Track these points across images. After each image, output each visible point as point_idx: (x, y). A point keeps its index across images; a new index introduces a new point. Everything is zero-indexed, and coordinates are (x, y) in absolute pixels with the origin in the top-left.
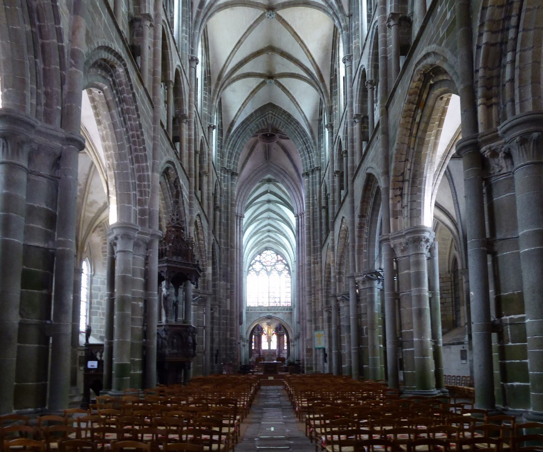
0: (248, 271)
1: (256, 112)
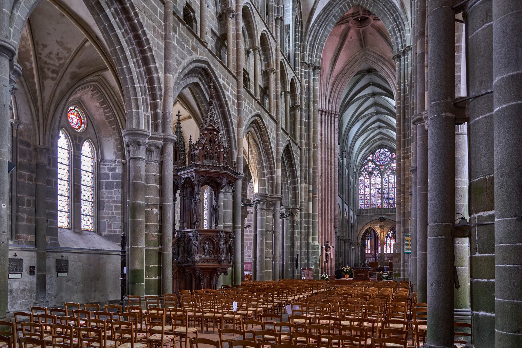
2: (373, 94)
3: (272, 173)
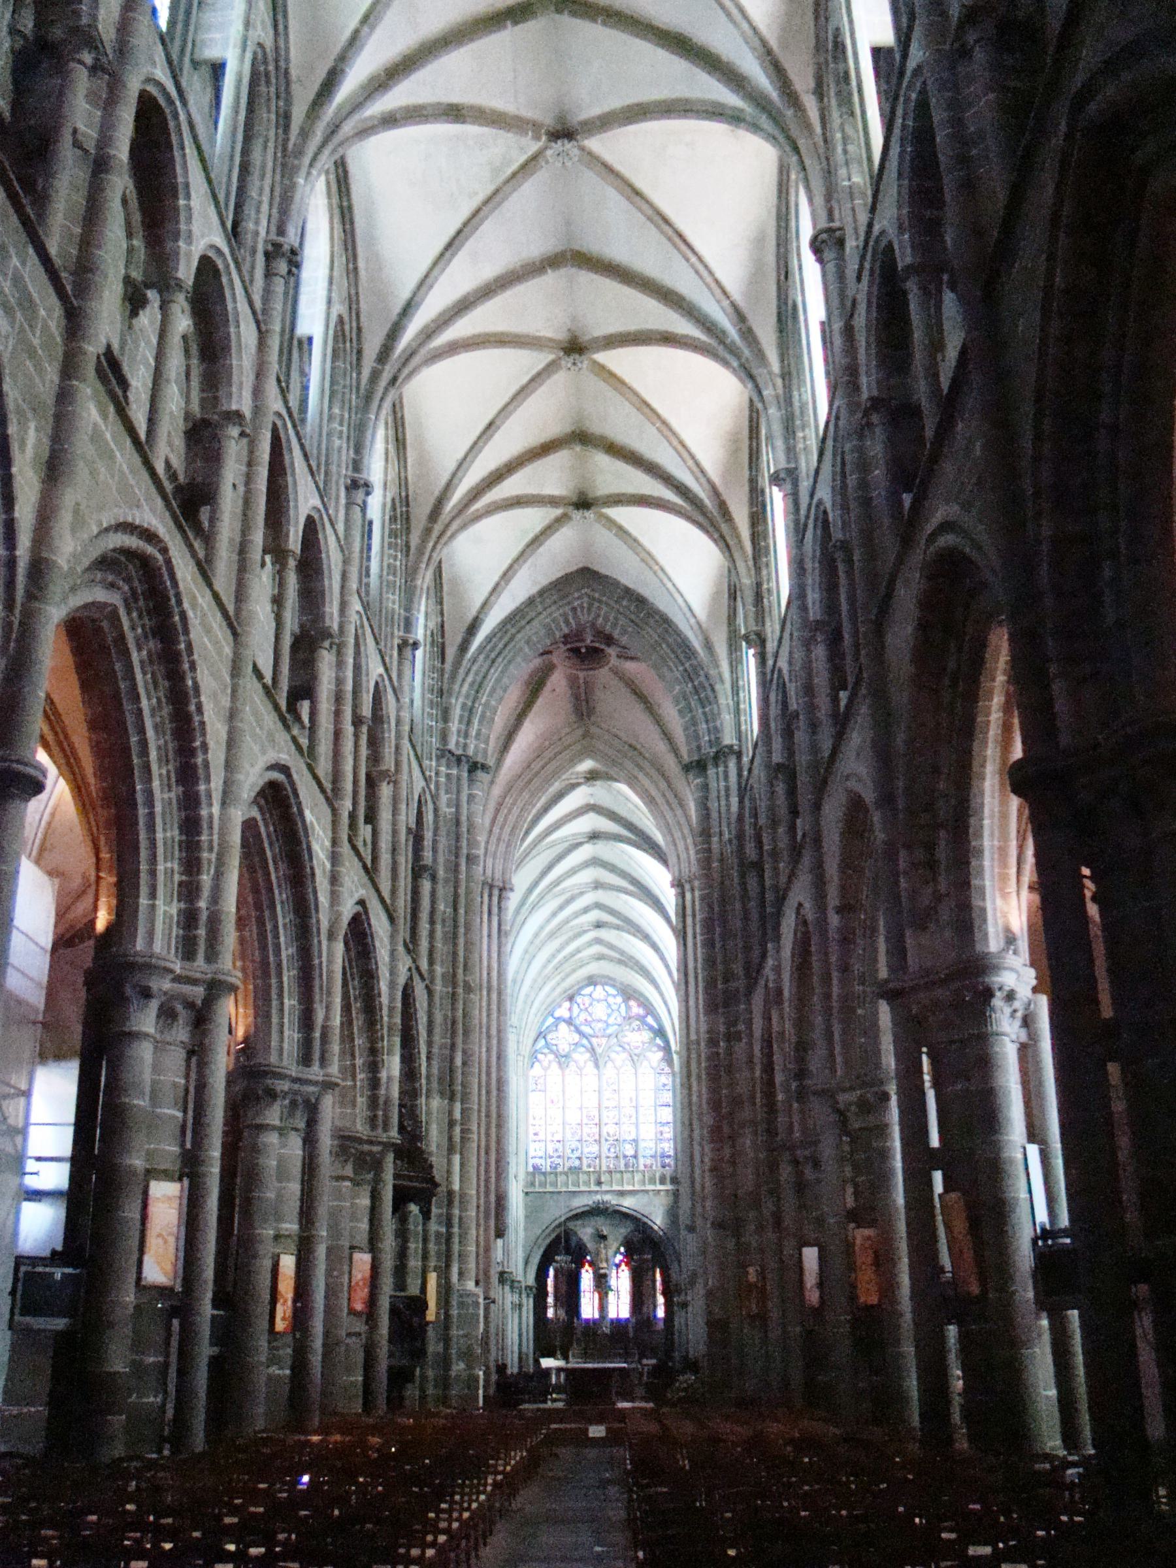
0: (534, 1057)
1: (542, 593)
2: (594, 836)
3: (374, 1067)
